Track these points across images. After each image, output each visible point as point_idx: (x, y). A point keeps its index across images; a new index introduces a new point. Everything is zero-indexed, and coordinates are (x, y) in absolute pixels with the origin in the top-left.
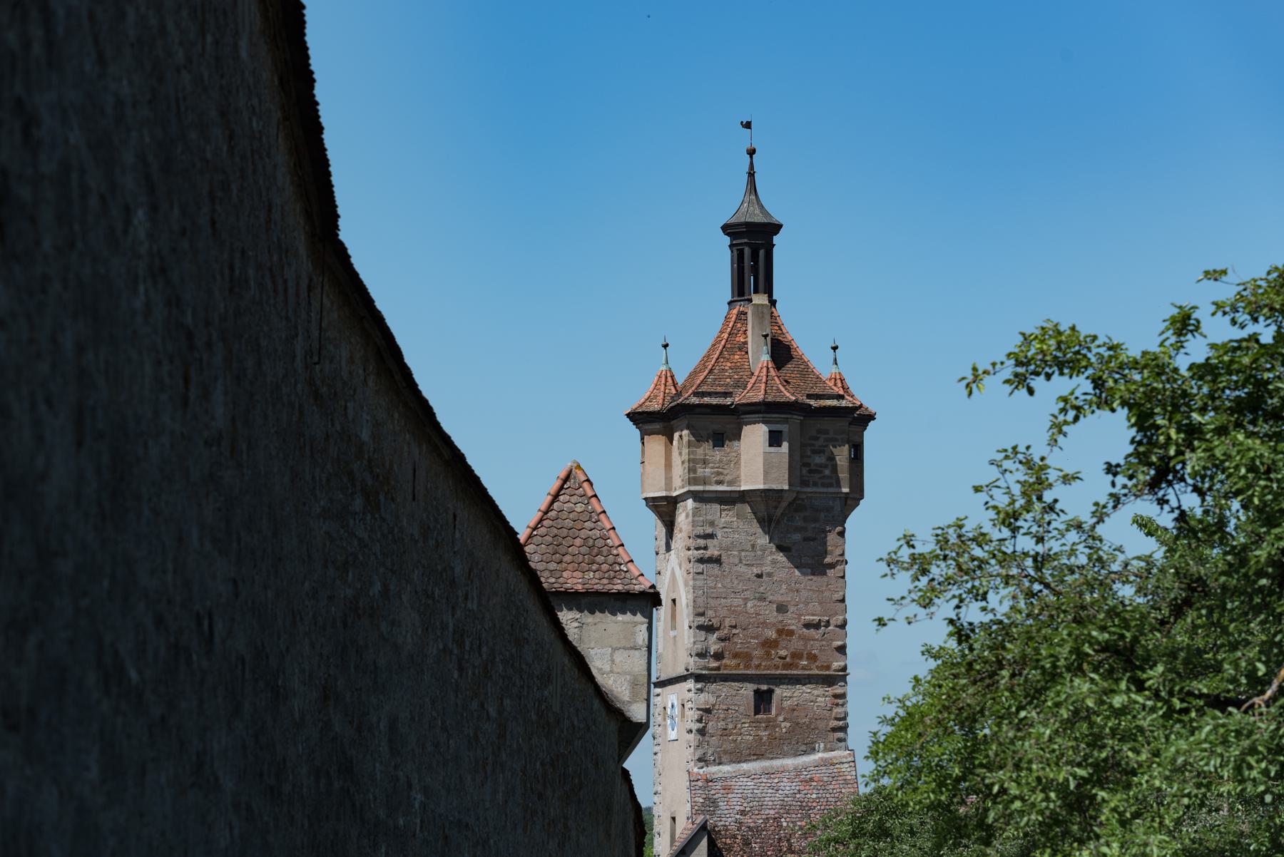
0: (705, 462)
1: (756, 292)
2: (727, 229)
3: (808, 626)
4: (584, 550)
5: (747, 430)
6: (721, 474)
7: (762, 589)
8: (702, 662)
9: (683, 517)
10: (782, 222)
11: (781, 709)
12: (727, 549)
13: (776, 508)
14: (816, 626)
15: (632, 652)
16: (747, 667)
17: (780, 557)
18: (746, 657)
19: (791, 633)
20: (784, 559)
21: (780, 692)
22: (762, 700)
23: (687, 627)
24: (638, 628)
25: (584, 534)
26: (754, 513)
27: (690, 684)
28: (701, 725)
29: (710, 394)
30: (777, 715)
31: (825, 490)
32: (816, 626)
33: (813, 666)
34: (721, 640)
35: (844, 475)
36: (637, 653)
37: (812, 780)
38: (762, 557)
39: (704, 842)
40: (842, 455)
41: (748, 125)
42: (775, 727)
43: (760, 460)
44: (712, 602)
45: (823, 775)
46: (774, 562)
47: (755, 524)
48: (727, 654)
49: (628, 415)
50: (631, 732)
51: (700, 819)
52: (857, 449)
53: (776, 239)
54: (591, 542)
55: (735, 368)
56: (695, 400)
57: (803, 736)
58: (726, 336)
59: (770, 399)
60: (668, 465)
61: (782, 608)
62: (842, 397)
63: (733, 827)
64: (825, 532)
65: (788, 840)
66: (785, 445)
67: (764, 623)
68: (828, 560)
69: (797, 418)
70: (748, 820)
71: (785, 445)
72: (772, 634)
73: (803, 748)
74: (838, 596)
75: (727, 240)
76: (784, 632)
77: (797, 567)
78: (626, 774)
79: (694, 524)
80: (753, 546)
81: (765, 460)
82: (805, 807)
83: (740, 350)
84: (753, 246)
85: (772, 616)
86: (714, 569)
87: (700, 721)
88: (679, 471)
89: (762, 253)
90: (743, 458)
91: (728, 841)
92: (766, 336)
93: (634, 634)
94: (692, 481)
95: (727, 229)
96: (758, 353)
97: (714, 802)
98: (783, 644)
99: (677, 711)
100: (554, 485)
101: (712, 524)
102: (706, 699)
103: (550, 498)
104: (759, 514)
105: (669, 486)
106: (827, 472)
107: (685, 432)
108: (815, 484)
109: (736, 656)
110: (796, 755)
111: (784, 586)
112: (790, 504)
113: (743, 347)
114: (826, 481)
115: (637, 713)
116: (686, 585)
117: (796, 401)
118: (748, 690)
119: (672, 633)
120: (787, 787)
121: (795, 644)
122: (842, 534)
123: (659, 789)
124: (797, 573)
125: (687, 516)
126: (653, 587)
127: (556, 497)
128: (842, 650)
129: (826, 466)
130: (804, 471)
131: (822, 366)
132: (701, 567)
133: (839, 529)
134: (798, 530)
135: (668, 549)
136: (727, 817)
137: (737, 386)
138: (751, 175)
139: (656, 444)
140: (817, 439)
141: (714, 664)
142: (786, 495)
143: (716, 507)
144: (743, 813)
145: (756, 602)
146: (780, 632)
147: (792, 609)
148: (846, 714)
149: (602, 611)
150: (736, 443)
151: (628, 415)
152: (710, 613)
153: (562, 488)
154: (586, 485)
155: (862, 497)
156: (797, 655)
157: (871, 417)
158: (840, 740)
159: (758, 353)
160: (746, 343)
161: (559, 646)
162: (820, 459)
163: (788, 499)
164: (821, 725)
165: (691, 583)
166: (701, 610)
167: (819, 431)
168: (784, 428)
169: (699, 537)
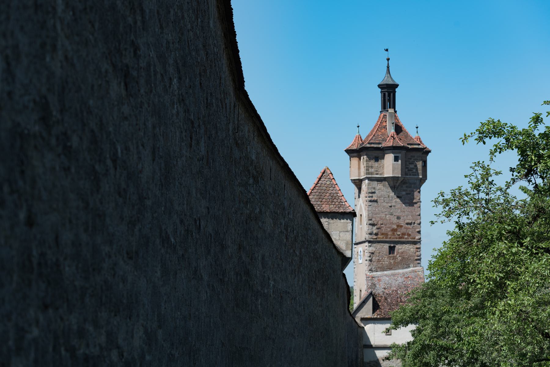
0: (372, 167)
1: (390, 108)
2: (380, 86)
3: (407, 224)
4: (330, 197)
5: (387, 156)
8: (371, 236)
10: (399, 83)
11: (398, 253)
14: (411, 224)
15: (346, 233)
16: (386, 238)
17: (398, 200)
18: (386, 235)
19: (402, 226)
21: (398, 247)
22: (392, 250)
24: (348, 224)
25: (330, 192)
27: (367, 244)
29: (374, 143)
32: (411, 224)
34: (378, 229)
35: (420, 172)
36: (348, 233)
37: (409, 277)
38: (392, 200)
39: (371, 299)
40: (419, 165)
41: (387, 50)
42: (396, 259)
44: (374, 216)
45: (412, 275)
46: (396, 202)
47: (389, 188)
48: (379, 234)
50: (346, 261)
51: (370, 291)
53: (397, 90)
54: (332, 195)
56: (368, 145)
57: (405, 262)
58: (379, 123)
59: (394, 145)
60: (359, 168)
61: (398, 218)
62: (420, 145)
63: (381, 293)
64: (414, 191)
66: (400, 161)
68: (414, 201)
69: (404, 152)
70: (386, 291)
71: (400, 161)
72: (395, 227)
74: (418, 214)
75: (380, 90)
76: (399, 226)
78: (344, 275)
79: (368, 188)
80: (389, 196)
82: (406, 287)
84: (389, 92)
85: (395, 220)
86: (375, 204)
87: (370, 257)
88: (363, 170)
89: (392, 94)
90: (385, 165)
93: (347, 226)
94: (367, 174)
95: (380, 86)
97: (375, 285)
98: (399, 230)
99: (362, 253)
100: (319, 175)
101: (374, 188)
102: (372, 249)
103: (318, 179)
105: (359, 175)
106: (414, 171)
107: (365, 157)
108: (410, 175)
109: (382, 234)
110: (403, 269)
112: (401, 182)
113: (385, 127)
115: (348, 254)
116: (365, 210)
117: (404, 146)
119: (360, 226)
120: (400, 280)
121: (403, 230)
122: (419, 192)
123: (356, 280)
124: (404, 205)
126: (354, 210)
127: (320, 179)
128: (419, 232)
129: (414, 169)
130: (407, 170)
131: (413, 134)
132: (370, 203)
133: (418, 190)
134: (404, 191)
135: (359, 197)
136: (379, 290)
137: (383, 140)
138: (388, 67)
139: (355, 161)
140: (411, 159)
143: (376, 182)
144: (385, 289)
146: (398, 226)
148: (421, 255)
149: (336, 219)
150: (383, 160)
152: (373, 219)
153: (322, 176)
154: (330, 175)
156: (403, 234)
157: (430, 152)
158: (418, 263)
161: (321, 231)
162: (412, 166)
164: (412, 258)
167: (412, 156)
169: (370, 193)
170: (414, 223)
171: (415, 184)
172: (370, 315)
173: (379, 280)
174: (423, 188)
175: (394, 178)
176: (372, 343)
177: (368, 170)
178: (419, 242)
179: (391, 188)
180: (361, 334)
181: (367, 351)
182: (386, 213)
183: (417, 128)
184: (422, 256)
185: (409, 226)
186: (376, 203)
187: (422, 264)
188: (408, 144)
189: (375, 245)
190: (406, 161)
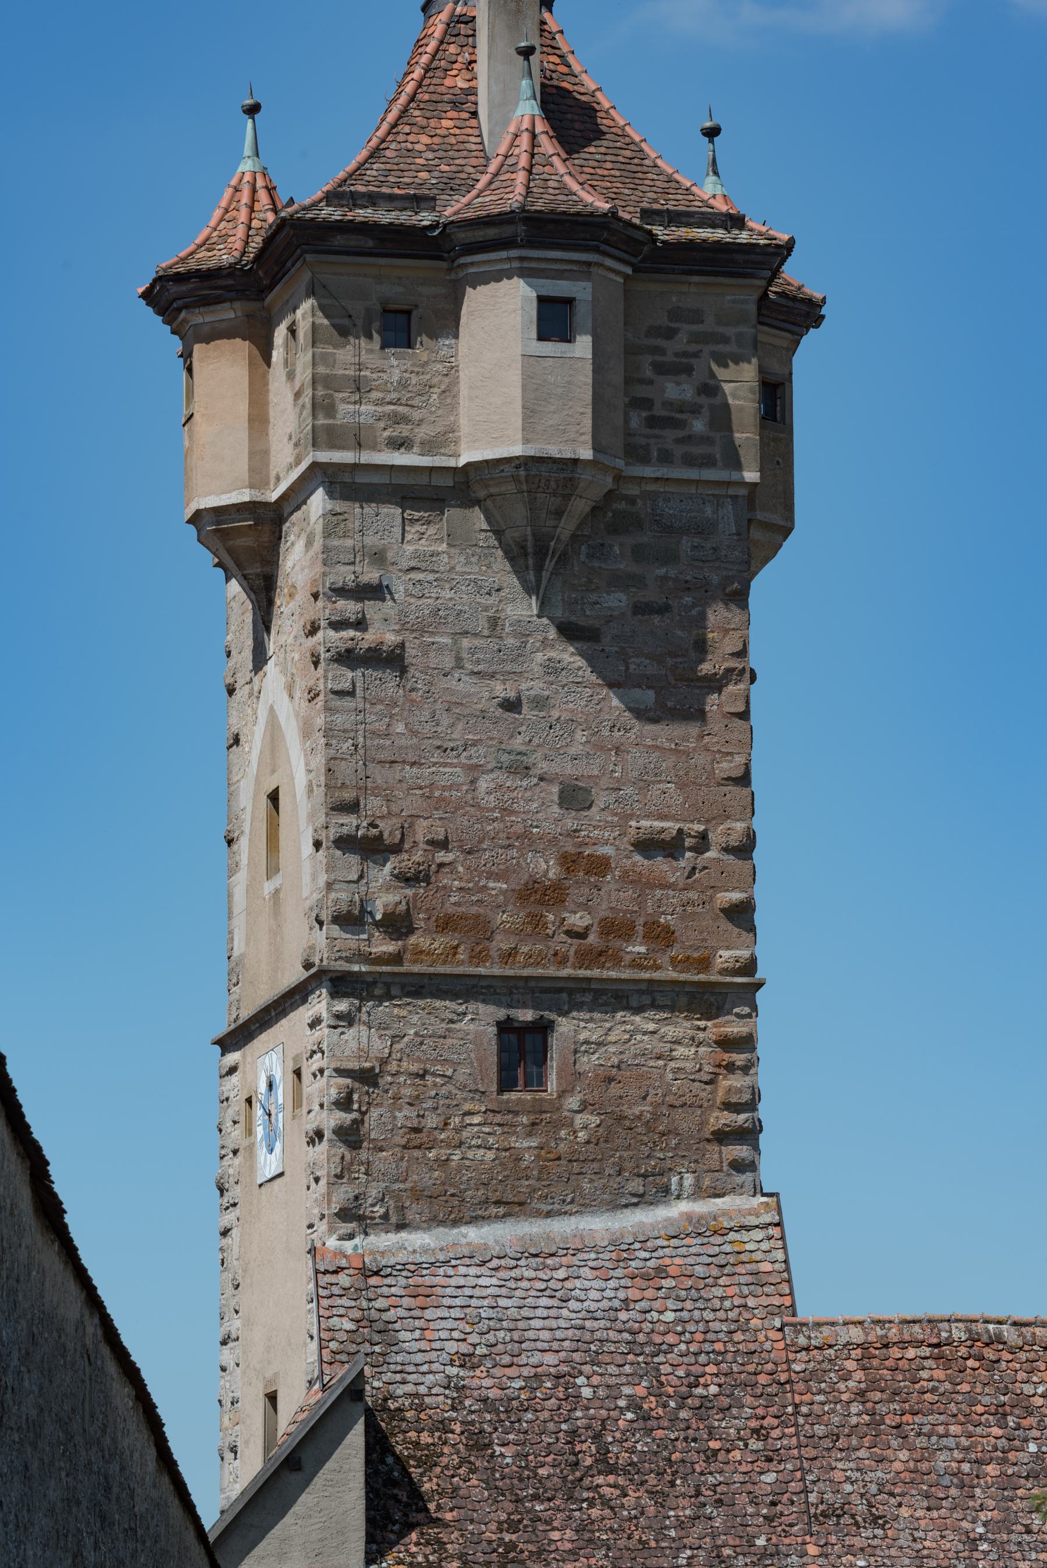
3: (647, 846)
6: (405, 420)
7: (518, 743)
8: (350, 941)
9: (298, 561)
11: (573, 1077)
12: (422, 630)
13: (559, 514)
14: (669, 847)
16: (478, 956)
17: (568, 655)
18: (479, 929)
19: (600, 866)
20: (580, 662)
21: (569, 1029)
22: (521, 1051)
23: (308, 848)
26: (498, 533)
28: (347, 1118)
29: (372, 200)
30: (562, 1094)
31: (692, 474)
32: (669, 847)
33: (663, 959)
34: (405, 879)
35: (746, 436)
37: (661, 1272)
38: (520, 654)
39: (356, 1437)
40: (739, 385)
43: (514, 378)
44: (380, 775)
45: (692, 1256)
46: (552, 669)
47: (500, 563)
48: (420, 919)
49: (147, 296)
51: (341, 1374)
52: (775, 397)
55: (444, 150)
56: (332, 213)
57: (634, 1155)
58: (418, 73)
60: (259, 419)
61: (574, 797)
63: (439, 1400)
65: (597, 1437)
66: (583, 346)
67: (525, 835)
68: (706, 668)
69: (615, 269)
70: (481, 1381)
71: (583, 346)
72: (546, 867)
73: (636, 1185)
77: (611, 685)
80: (494, 623)
81: (527, 378)
82: (644, 1348)
83: (456, 105)
85: (546, 814)
86: (385, 684)
87: (344, 1103)
90: (465, 375)
91: (425, 1438)
92: (527, 52)
98: (577, 894)
101: (378, 557)
102: (360, 1043)
104: (510, 535)
105: (258, 475)
108: (665, 458)
109: (445, 924)
110: (615, 1206)
111: (580, 736)
113: (464, 102)
114: (697, 450)
116: (306, 733)
117: (613, 214)
119: (268, 887)
120: (593, 1292)
121: (613, 897)
122: (740, 598)
123: (235, 1325)
125: (309, 544)
128: (742, 914)
129: (695, 410)
130: (636, 421)
132: (346, 677)
134: (618, 582)
135: (260, 658)
136: (420, 1372)
139: (223, 366)
140: (670, 334)
141: (385, 947)
142: (585, 476)
143: (392, 512)
144: (466, 1361)
145: (501, 777)
146: (569, 862)
151: (147, 296)
152: (373, 804)
155: (786, 531)
156: (616, 928)
158: (740, 1166)
159: (504, 105)
160: (472, 91)
162: (677, 390)
163: (595, 486)
164: (686, 1121)
165: (320, 721)
166: (348, 795)
167: (675, 314)
168: (580, 290)
169: (341, 592)
170: (703, 842)
171: (703, 529)
173: (423, 1295)
174: (764, 586)
175: (537, 476)
177: (330, 410)
178: (741, 989)
179: (516, 555)
182: (478, 754)
183: (712, 133)
184: (764, 1111)
185: (661, 865)
186: (389, 676)
187: (769, 1175)
188: (646, 214)
189: (384, 1010)
190: (631, 351)
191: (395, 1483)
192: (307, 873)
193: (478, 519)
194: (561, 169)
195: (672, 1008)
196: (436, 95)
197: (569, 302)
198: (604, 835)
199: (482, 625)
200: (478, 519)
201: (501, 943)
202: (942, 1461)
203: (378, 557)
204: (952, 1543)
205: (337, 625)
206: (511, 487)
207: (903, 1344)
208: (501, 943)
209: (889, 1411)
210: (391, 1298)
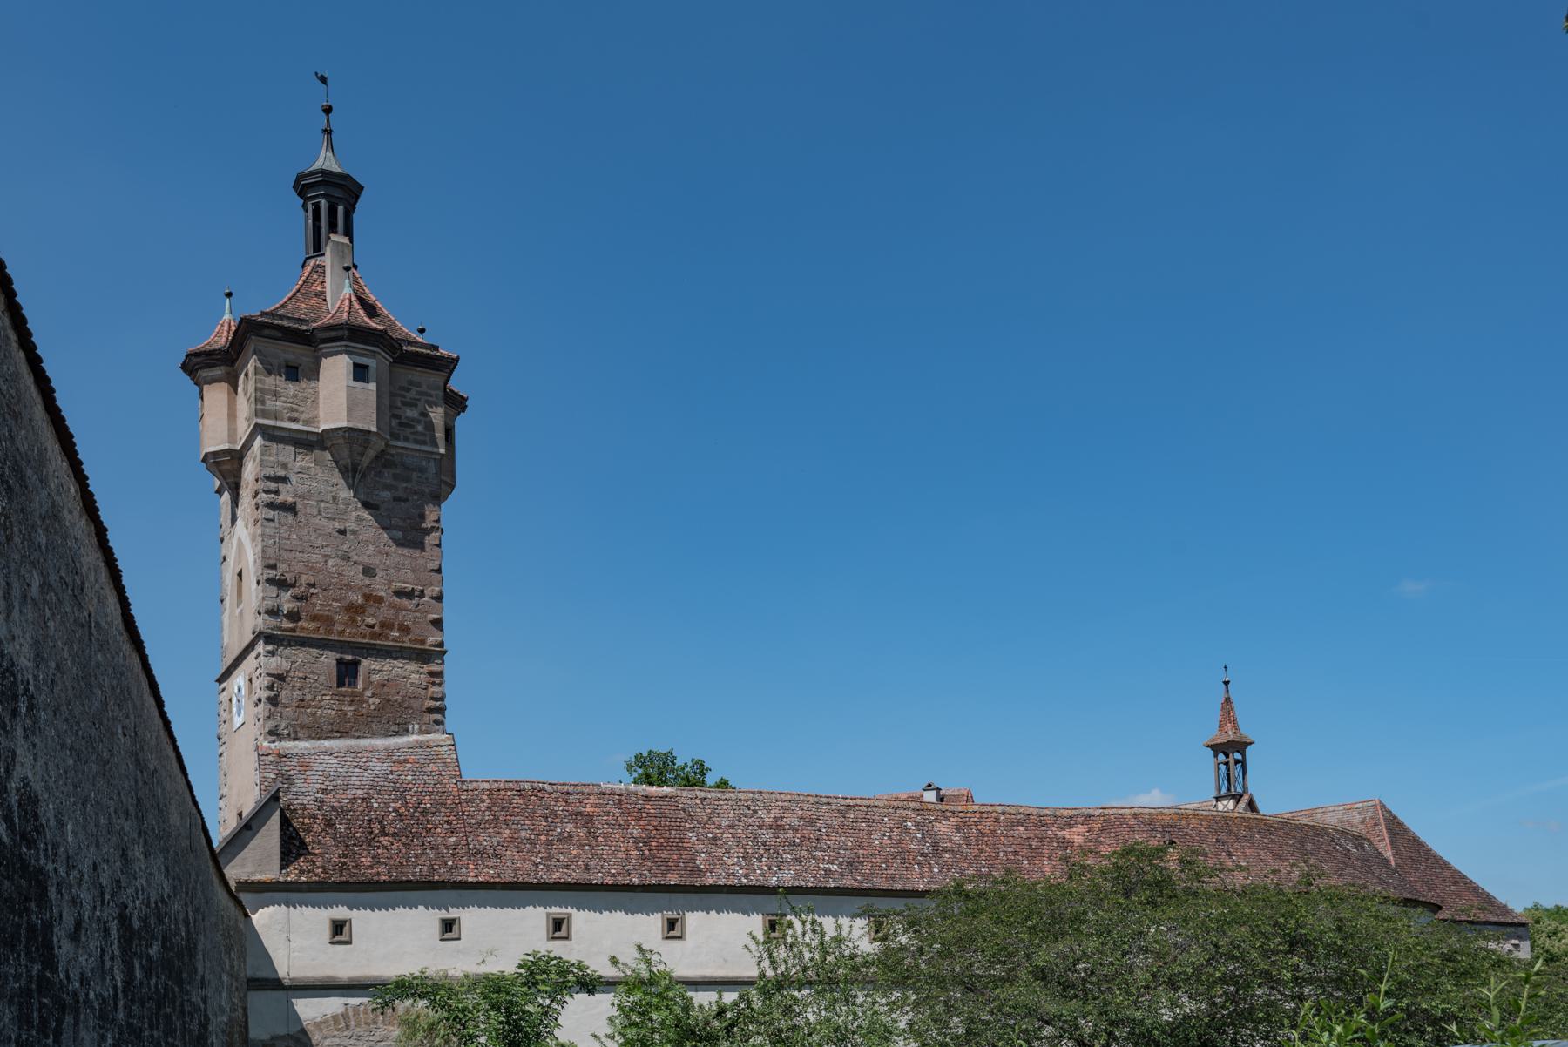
7: (345, 547)
8: (272, 621)
13: (362, 454)
17: (365, 514)
18: (328, 621)
19: (380, 600)
21: (366, 664)
22: (347, 672)
34: (297, 598)
37: (406, 761)
39: (276, 817)
48: (303, 615)
55: (312, 309)
61: (368, 571)
63: (313, 807)
66: (372, 386)
67: (348, 585)
70: (331, 800)
72: (357, 598)
76: (372, 599)
79: (262, 464)
80: (335, 498)
82: (400, 790)
84: (332, 200)
87: (271, 687)
92: (347, 269)
96: (338, 289)
98: (370, 610)
102: (277, 663)
104: (342, 462)
109: (314, 618)
110: (386, 736)
111: (371, 547)
113: (321, 295)
116: (253, 540)
117: (385, 331)
118: (329, 659)
120: (377, 767)
121: (385, 612)
132: (271, 514)
136: (304, 793)
138: (328, 132)
142: (374, 439)
144: (324, 791)
146: (367, 597)
147: (380, 573)
150: (313, 384)
152: (283, 567)
158: (437, 722)
164: (415, 704)
165: (259, 531)
166: (272, 562)
169: (268, 478)
172: (271, 872)
176: (282, 973)
179: (344, 471)
180: (245, 941)
181: (259, 1001)
182: (328, 551)
184: (447, 702)
186: (290, 518)
191: (291, 838)
192: (254, 594)
193: (328, 455)
194: (362, 313)
195: (410, 659)
196: (310, 290)
197: (366, 367)
198: (380, 587)
199: (330, 499)
200: (328, 455)
201: (338, 627)
202: (523, 834)
203: (285, 466)
204: (528, 865)
205: (267, 492)
206: (341, 441)
207: (506, 790)
208: (338, 627)
209: (501, 815)
210: (291, 766)
